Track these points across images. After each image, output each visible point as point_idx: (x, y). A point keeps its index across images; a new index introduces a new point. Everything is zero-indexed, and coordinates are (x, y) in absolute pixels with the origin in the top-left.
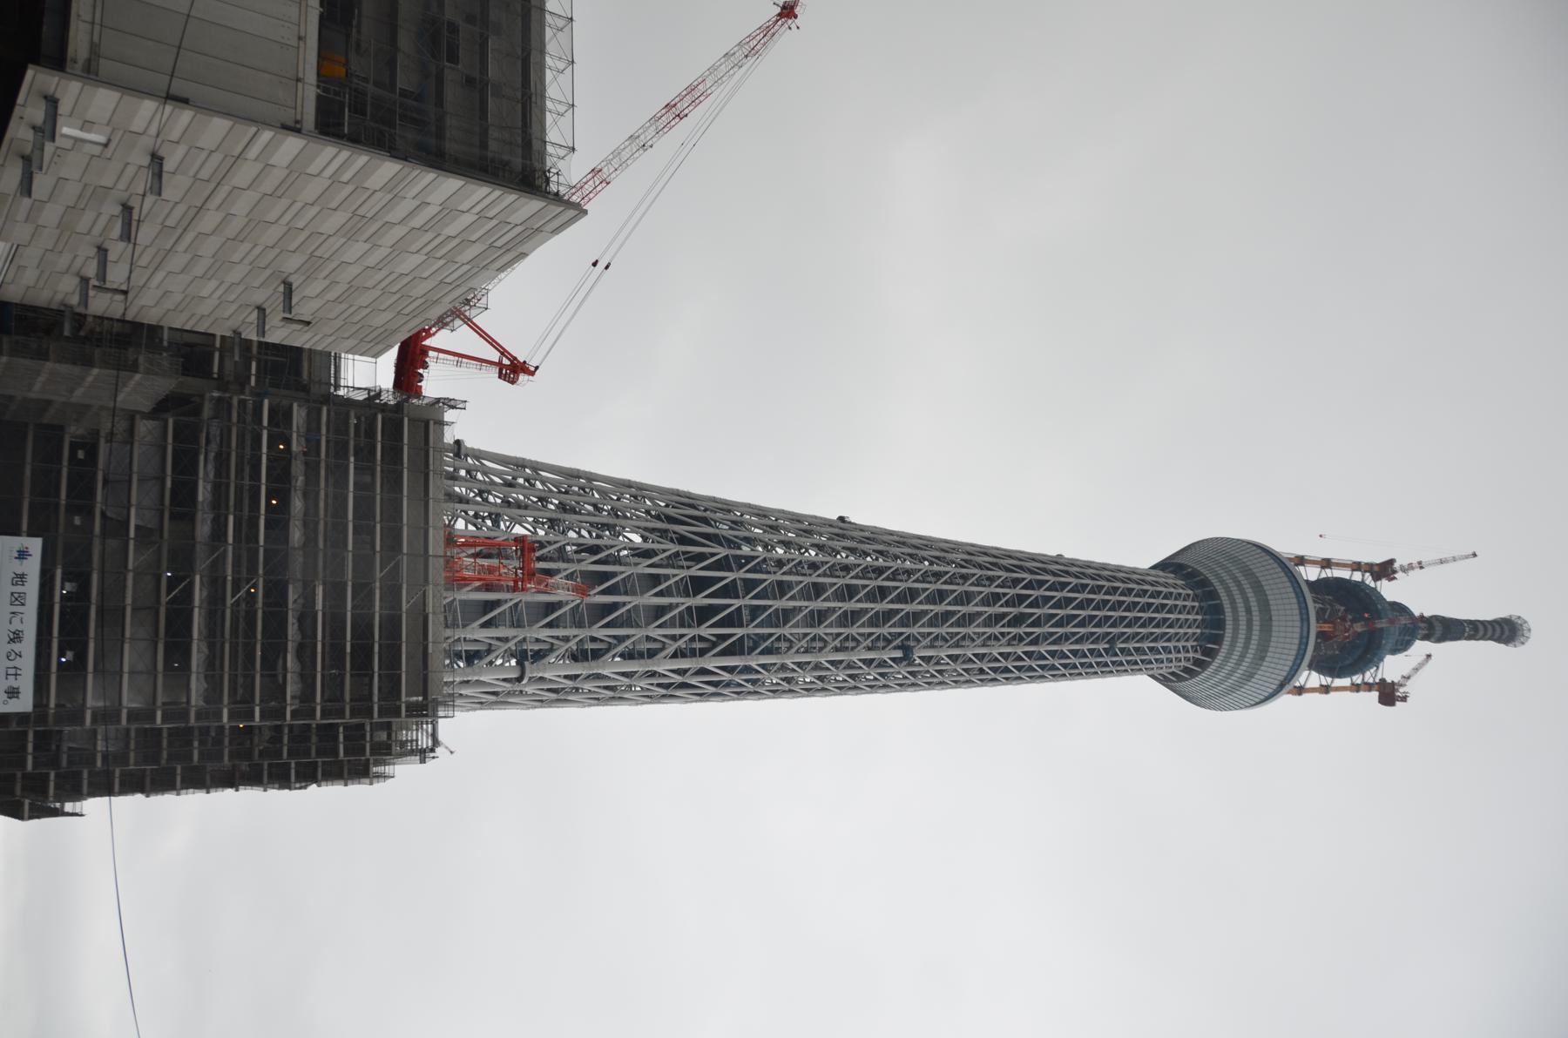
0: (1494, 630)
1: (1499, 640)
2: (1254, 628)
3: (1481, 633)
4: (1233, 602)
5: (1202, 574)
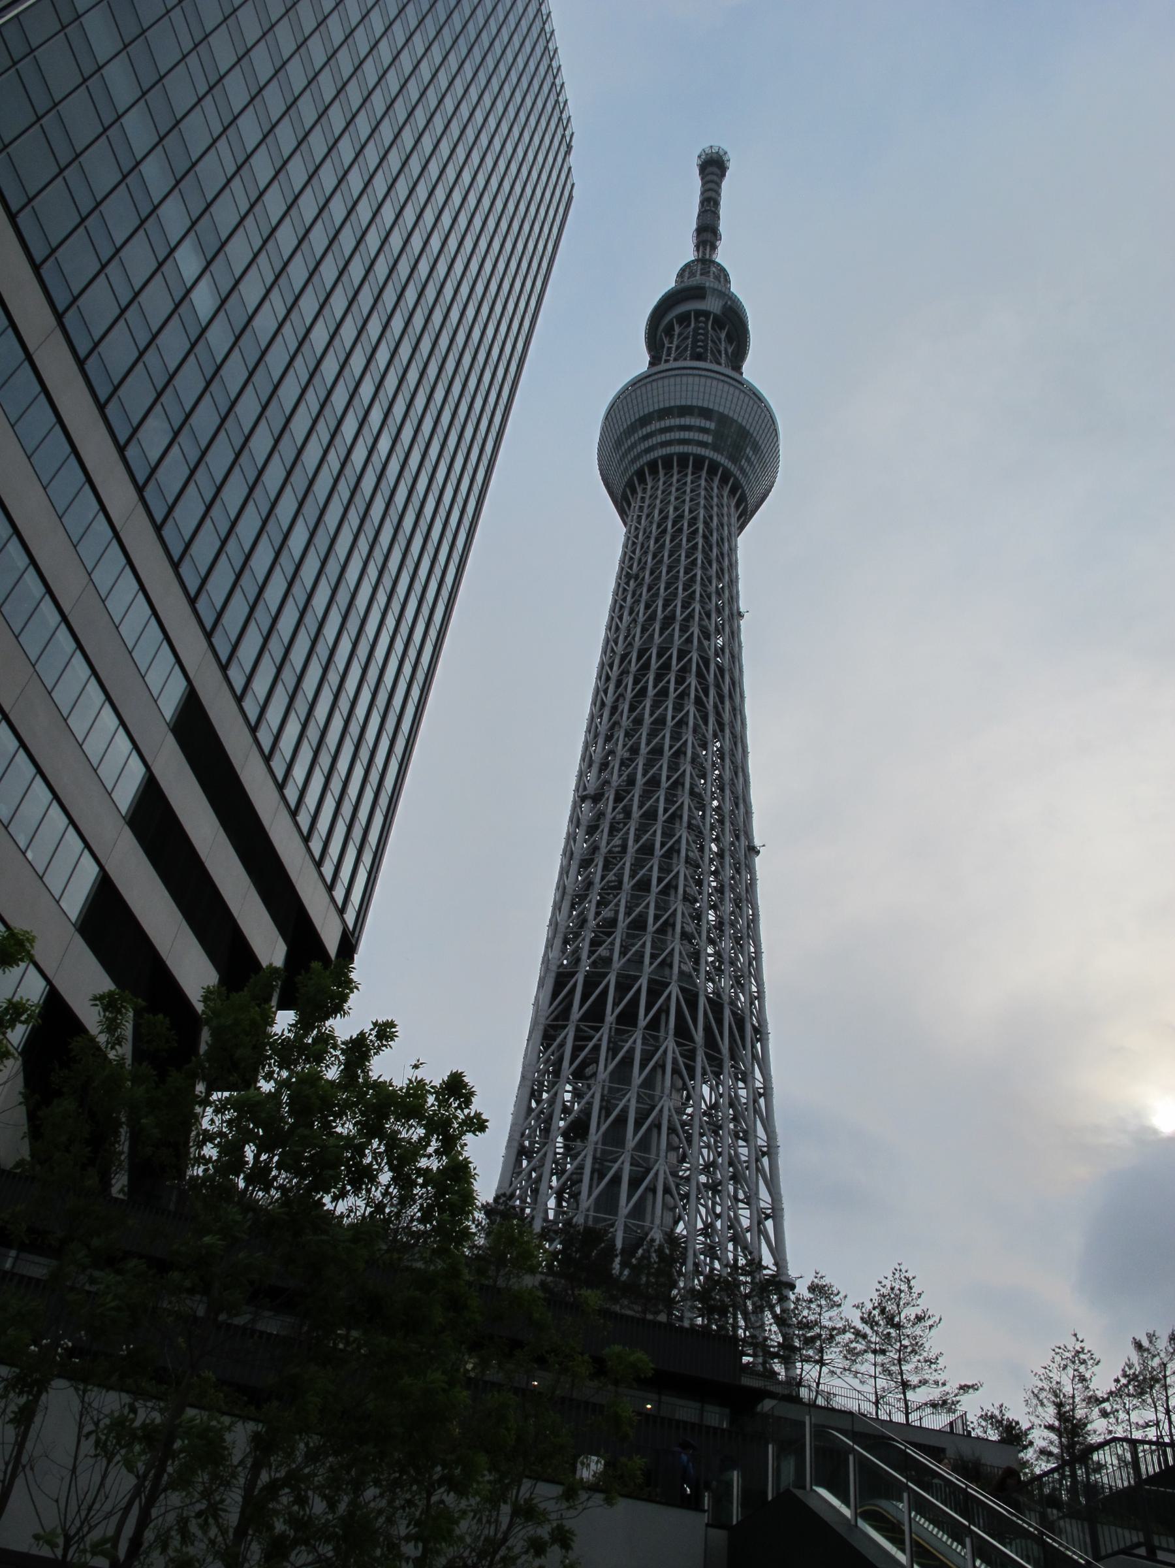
0: (712, 181)
1: (723, 175)
2: (688, 423)
3: (713, 194)
4: (664, 444)
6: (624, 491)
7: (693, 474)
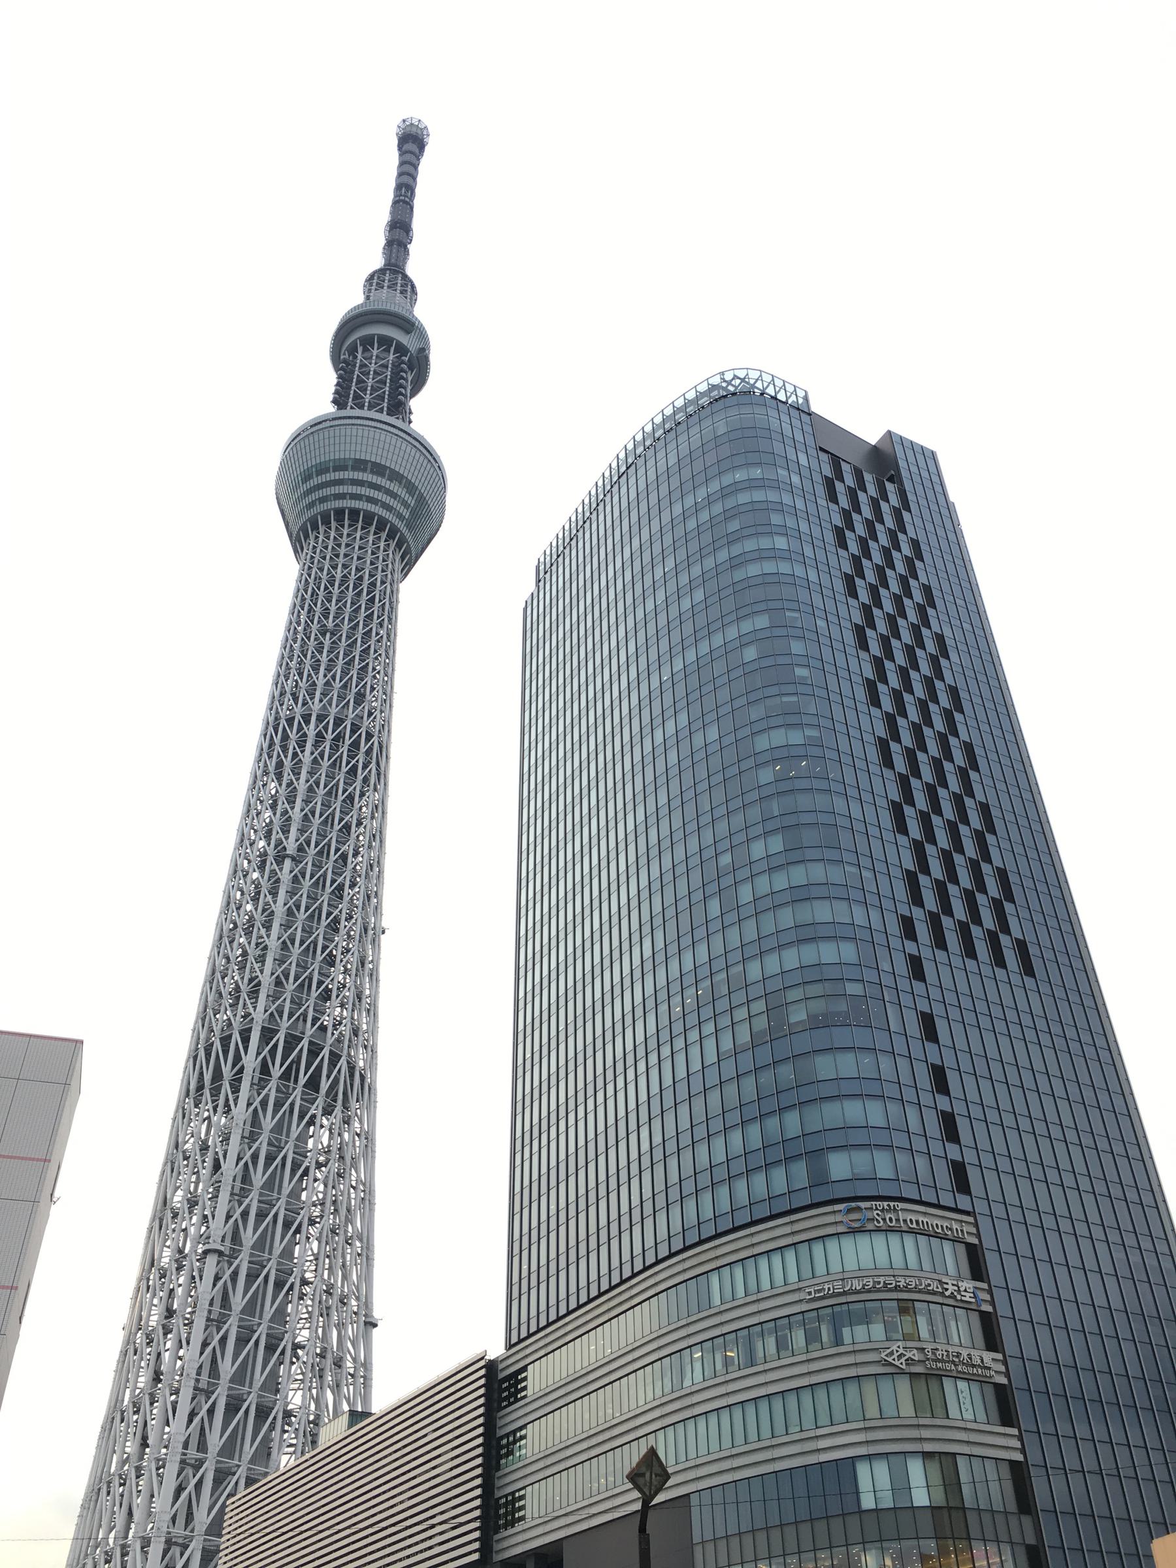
5: (305, 523)
6: (298, 532)
7: (363, 528)
